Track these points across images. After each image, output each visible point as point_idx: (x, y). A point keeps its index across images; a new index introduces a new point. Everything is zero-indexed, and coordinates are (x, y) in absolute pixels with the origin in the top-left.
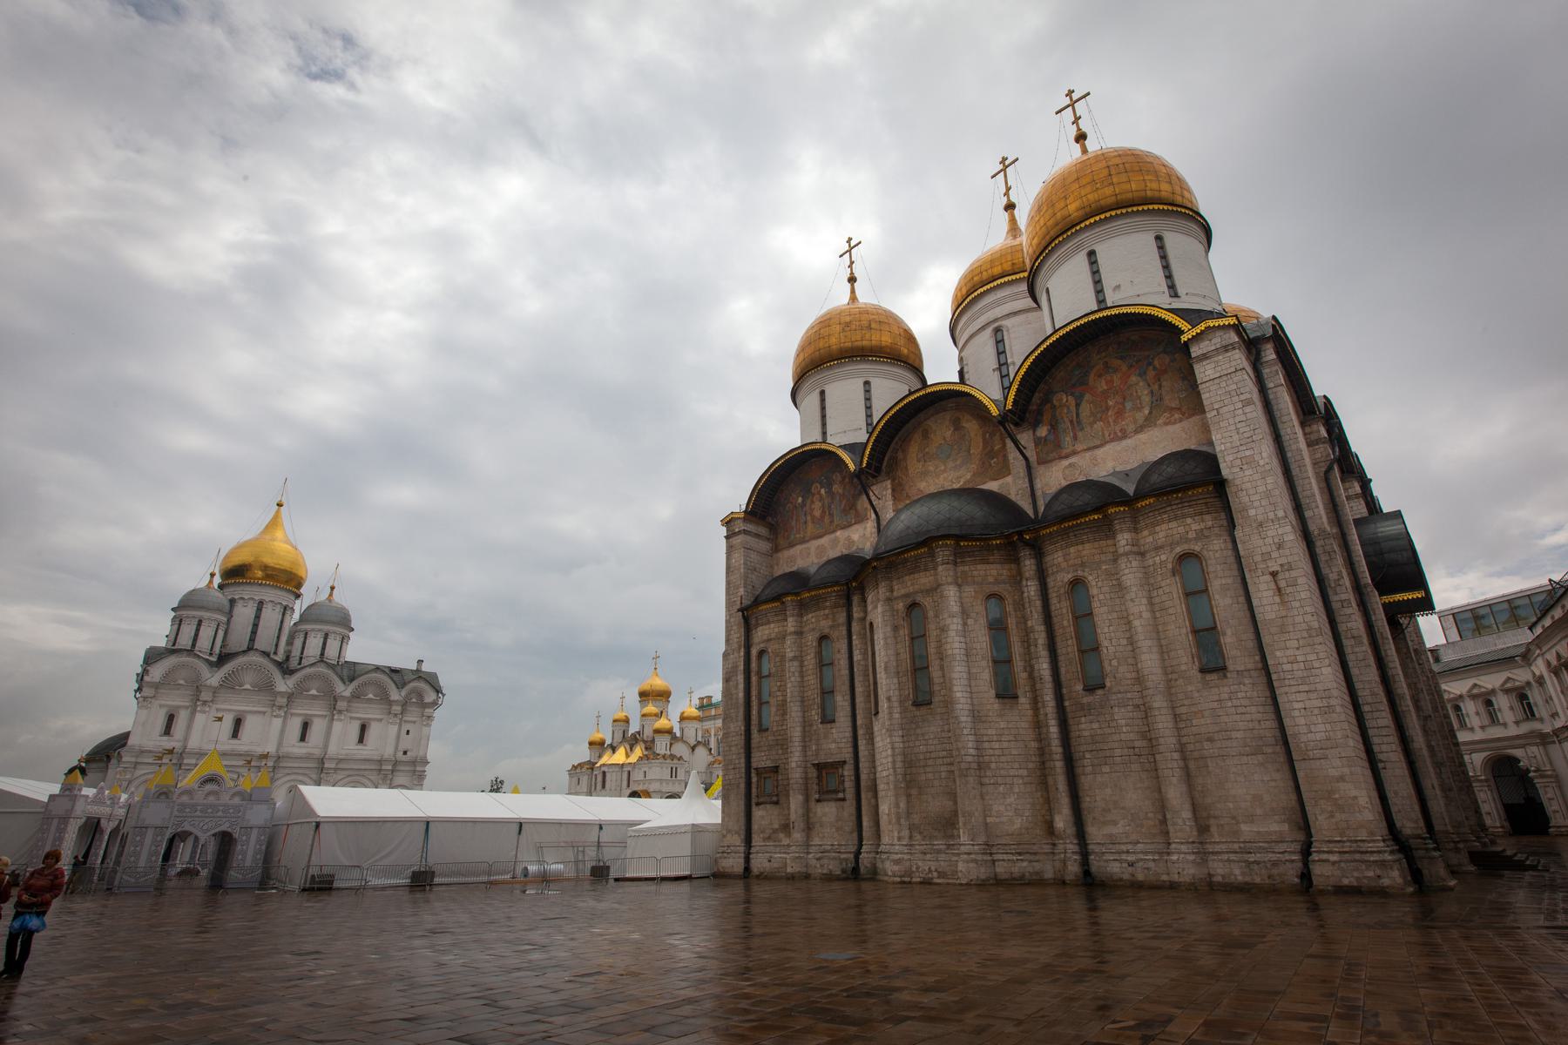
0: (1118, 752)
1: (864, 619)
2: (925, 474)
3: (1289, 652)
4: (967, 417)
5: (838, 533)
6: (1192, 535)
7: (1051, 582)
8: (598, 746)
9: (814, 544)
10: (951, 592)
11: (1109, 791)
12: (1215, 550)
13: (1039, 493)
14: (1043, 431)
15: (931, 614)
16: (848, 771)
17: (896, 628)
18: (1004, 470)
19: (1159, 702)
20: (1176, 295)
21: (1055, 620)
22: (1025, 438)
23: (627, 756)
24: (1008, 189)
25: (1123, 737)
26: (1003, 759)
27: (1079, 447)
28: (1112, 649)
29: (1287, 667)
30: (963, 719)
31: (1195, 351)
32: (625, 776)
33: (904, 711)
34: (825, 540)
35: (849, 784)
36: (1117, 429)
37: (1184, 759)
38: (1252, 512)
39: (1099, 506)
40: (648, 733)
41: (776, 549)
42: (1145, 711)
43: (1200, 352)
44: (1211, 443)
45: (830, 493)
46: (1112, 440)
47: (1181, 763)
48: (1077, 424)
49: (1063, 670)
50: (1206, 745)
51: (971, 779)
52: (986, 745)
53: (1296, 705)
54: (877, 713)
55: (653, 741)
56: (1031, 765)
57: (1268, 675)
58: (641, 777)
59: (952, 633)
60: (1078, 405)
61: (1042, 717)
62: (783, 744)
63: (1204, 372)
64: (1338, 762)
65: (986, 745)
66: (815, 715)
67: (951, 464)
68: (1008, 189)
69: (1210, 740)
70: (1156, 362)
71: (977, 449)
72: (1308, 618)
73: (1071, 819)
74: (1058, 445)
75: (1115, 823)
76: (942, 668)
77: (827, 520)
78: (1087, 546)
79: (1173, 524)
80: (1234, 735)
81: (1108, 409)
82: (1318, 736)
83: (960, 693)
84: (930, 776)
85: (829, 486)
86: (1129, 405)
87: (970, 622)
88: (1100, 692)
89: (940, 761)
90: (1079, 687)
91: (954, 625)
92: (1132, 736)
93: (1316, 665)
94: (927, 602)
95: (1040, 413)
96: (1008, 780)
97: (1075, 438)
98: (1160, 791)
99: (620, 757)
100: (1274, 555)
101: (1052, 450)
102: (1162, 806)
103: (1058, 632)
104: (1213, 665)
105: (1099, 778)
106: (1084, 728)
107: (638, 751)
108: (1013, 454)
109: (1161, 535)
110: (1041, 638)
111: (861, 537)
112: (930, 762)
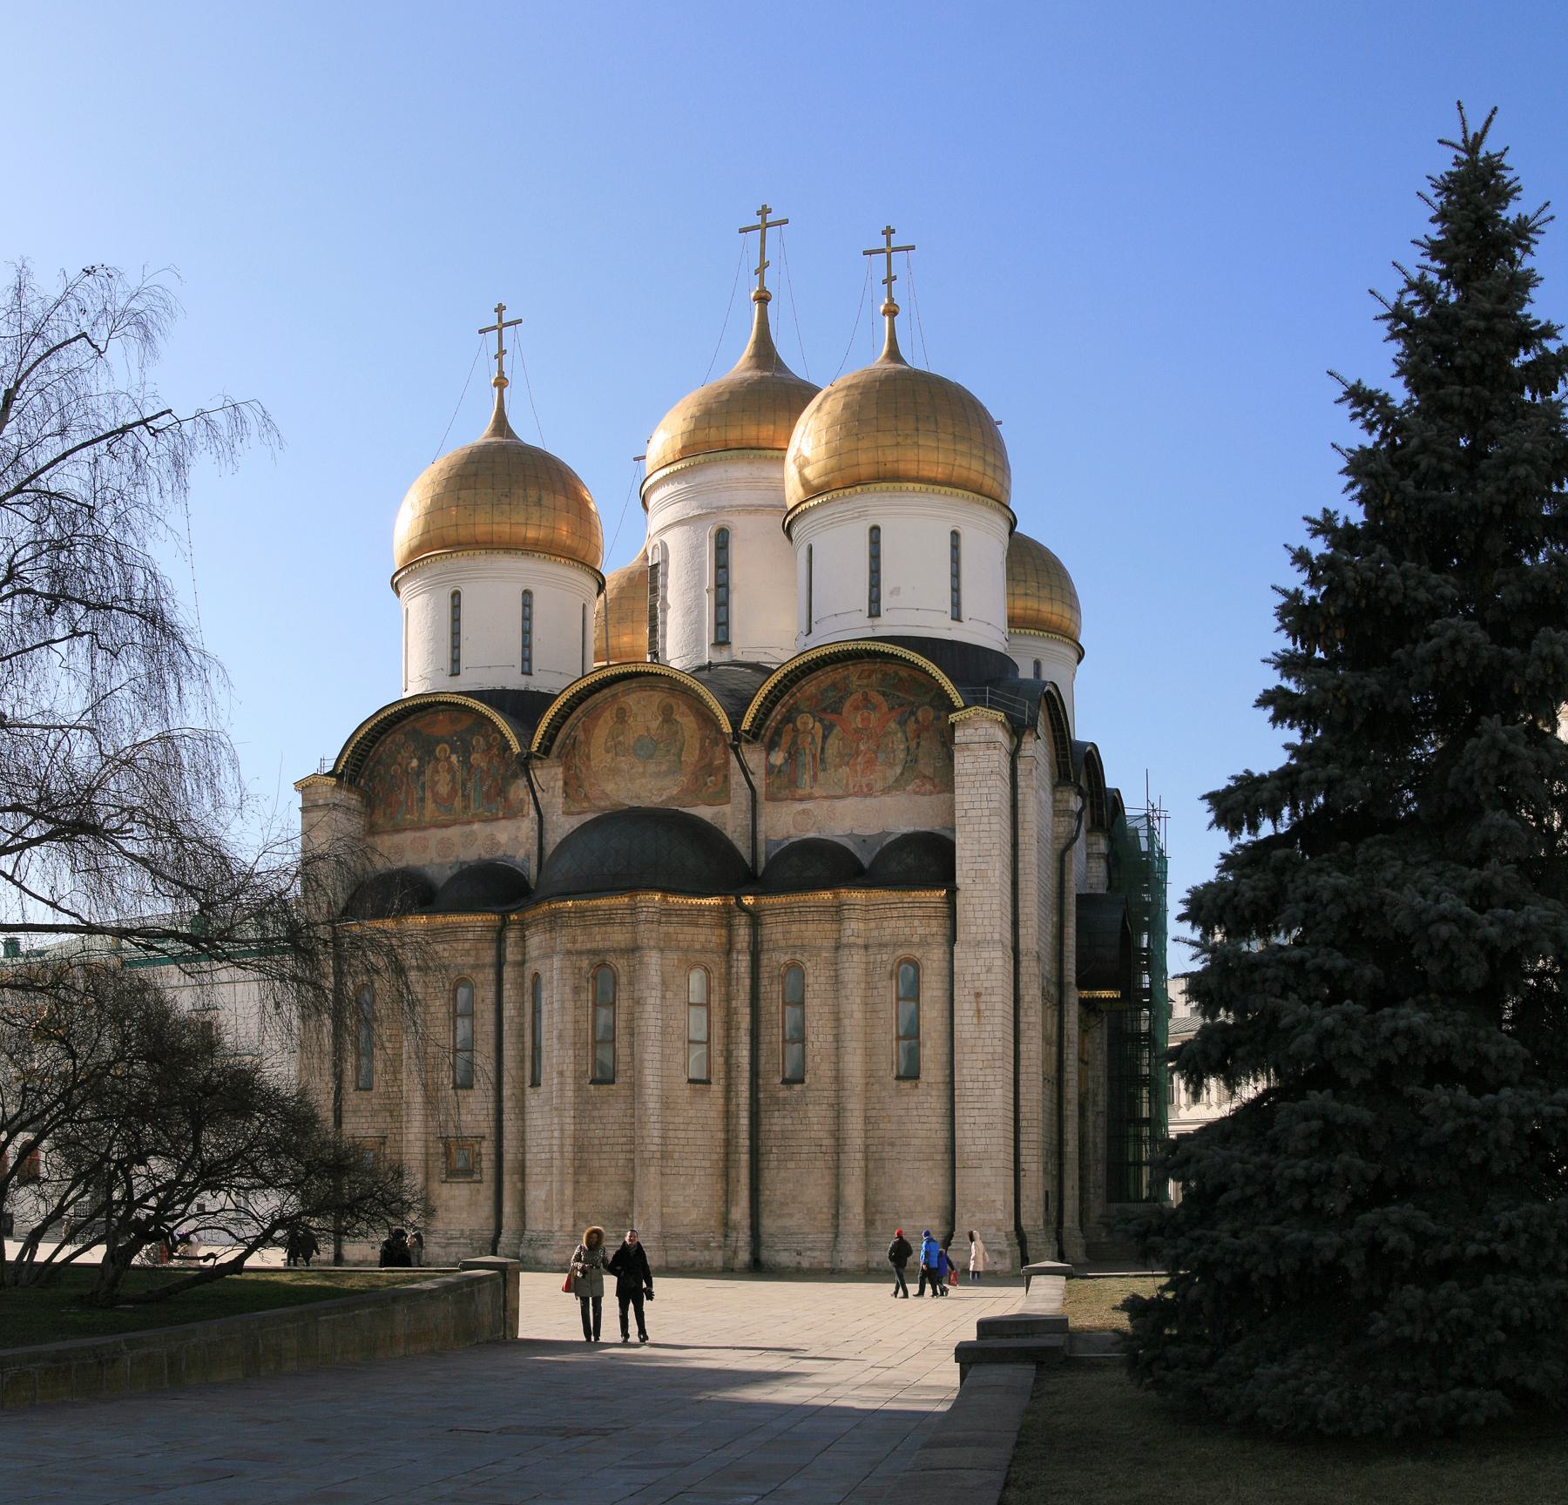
0: (805, 1149)
1: (522, 963)
2: (614, 771)
3: (974, 1072)
4: (683, 708)
5: (476, 826)
6: (916, 939)
7: (764, 959)
9: (435, 835)
10: (653, 959)
11: (791, 1186)
12: (933, 961)
13: (761, 837)
14: (778, 758)
15: (623, 980)
16: (487, 1148)
17: (576, 990)
18: (722, 795)
19: (854, 1106)
20: (957, 617)
21: (763, 1003)
22: (754, 757)
24: (764, 265)
25: (813, 1134)
26: (687, 1149)
27: (817, 791)
28: (817, 1045)
29: (969, 1085)
30: (651, 1105)
31: (959, 735)
33: (579, 1089)
34: (453, 832)
35: (487, 1164)
36: (864, 782)
37: (866, 1159)
38: (973, 929)
39: (825, 866)
41: (372, 830)
42: (839, 1110)
43: (964, 739)
44: (953, 830)
45: (465, 762)
46: (855, 794)
47: (862, 1163)
48: (821, 761)
49: (763, 1060)
50: (887, 1148)
51: (652, 1169)
52: (671, 1134)
53: (969, 1120)
54: (535, 1083)
56: (715, 1157)
57: (953, 1089)
59: (649, 1008)
60: (825, 738)
61: (732, 1108)
62: (394, 1108)
63: (962, 762)
64: (987, 1172)
65: (671, 1134)
66: (445, 1078)
67: (652, 768)
68: (764, 265)
69: (892, 1144)
70: (919, 713)
71: (691, 756)
72: (996, 1042)
73: (747, 1211)
74: (793, 783)
75: (791, 1215)
76: (631, 1046)
77: (458, 803)
78: (811, 927)
79: (901, 923)
80: (914, 1141)
81: (857, 753)
82: (980, 1148)
83: (651, 1078)
84: (605, 1163)
85: (465, 751)
86: (881, 757)
87: (669, 995)
88: (798, 1087)
89: (618, 1148)
90: (778, 1080)
91: (652, 999)
92: (821, 1134)
93: (992, 1085)
94: (620, 964)
95: (778, 732)
96: (690, 1171)
97: (815, 777)
98: (838, 1187)
100: (983, 977)
101: (785, 783)
102: (837, 1202)
103: (764, 1017)
104: (910, 1073)
105: (783, 1174)
106: (775, 1122)
108: (737, 778)
109: (888, 931)
110: (744, 1021)
111: (511, 839)
112: (606, 1148)
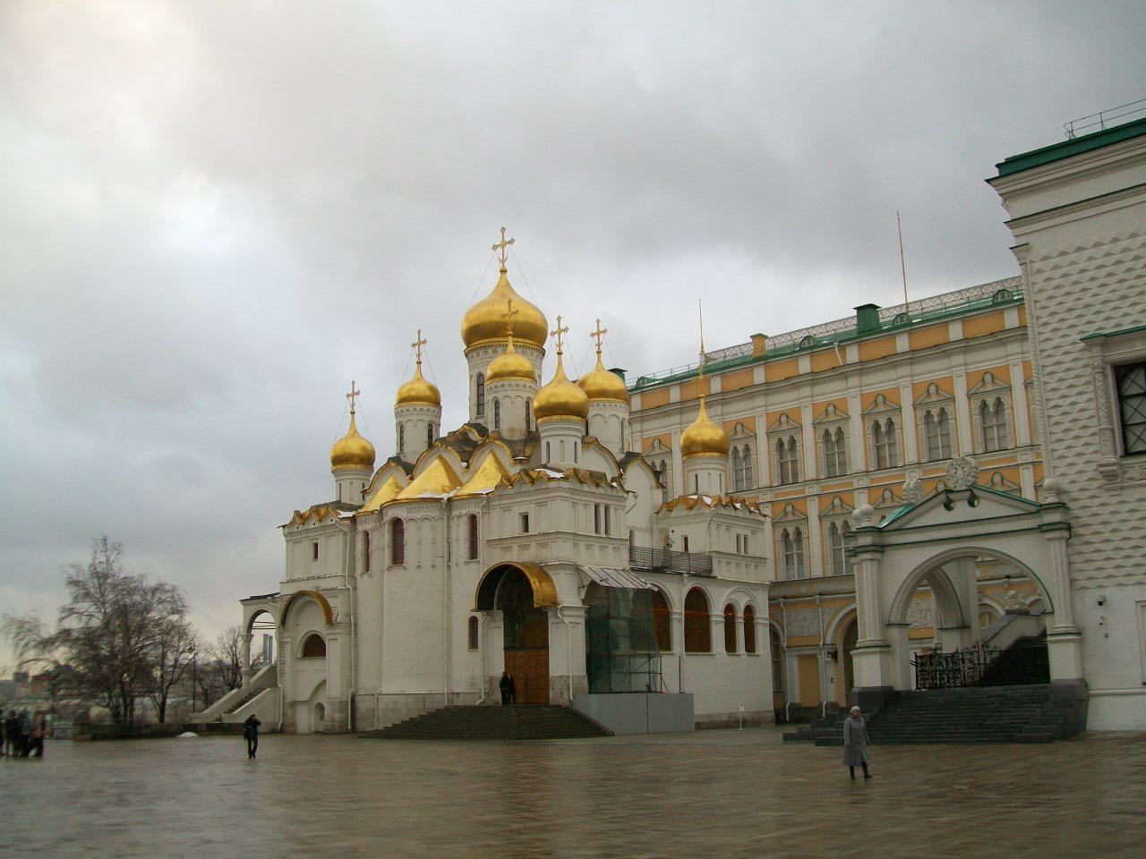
8: (352, 462)
23: (456, 481)
32: (461, 530)
40: (512, 420)
55: (532, 438)
58: (513, 526)
99: (432, 480)
107: (485, 476)
